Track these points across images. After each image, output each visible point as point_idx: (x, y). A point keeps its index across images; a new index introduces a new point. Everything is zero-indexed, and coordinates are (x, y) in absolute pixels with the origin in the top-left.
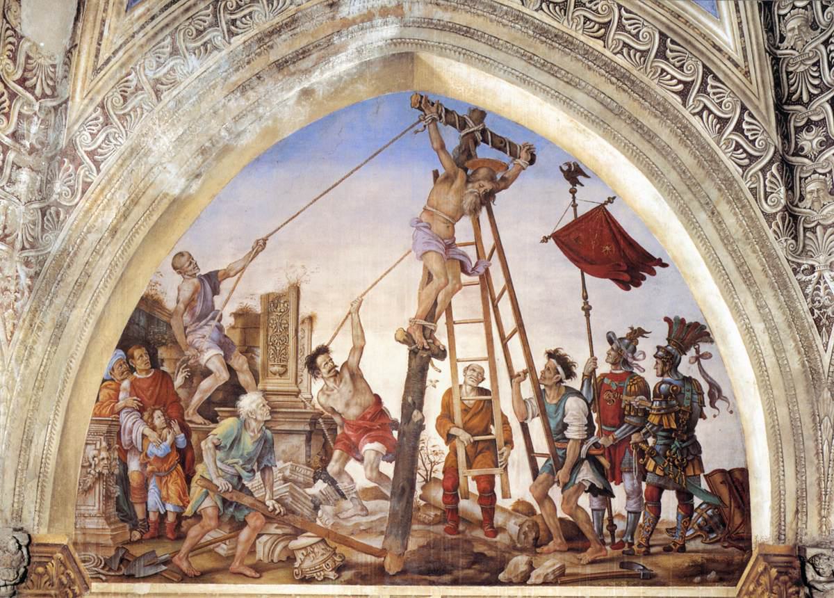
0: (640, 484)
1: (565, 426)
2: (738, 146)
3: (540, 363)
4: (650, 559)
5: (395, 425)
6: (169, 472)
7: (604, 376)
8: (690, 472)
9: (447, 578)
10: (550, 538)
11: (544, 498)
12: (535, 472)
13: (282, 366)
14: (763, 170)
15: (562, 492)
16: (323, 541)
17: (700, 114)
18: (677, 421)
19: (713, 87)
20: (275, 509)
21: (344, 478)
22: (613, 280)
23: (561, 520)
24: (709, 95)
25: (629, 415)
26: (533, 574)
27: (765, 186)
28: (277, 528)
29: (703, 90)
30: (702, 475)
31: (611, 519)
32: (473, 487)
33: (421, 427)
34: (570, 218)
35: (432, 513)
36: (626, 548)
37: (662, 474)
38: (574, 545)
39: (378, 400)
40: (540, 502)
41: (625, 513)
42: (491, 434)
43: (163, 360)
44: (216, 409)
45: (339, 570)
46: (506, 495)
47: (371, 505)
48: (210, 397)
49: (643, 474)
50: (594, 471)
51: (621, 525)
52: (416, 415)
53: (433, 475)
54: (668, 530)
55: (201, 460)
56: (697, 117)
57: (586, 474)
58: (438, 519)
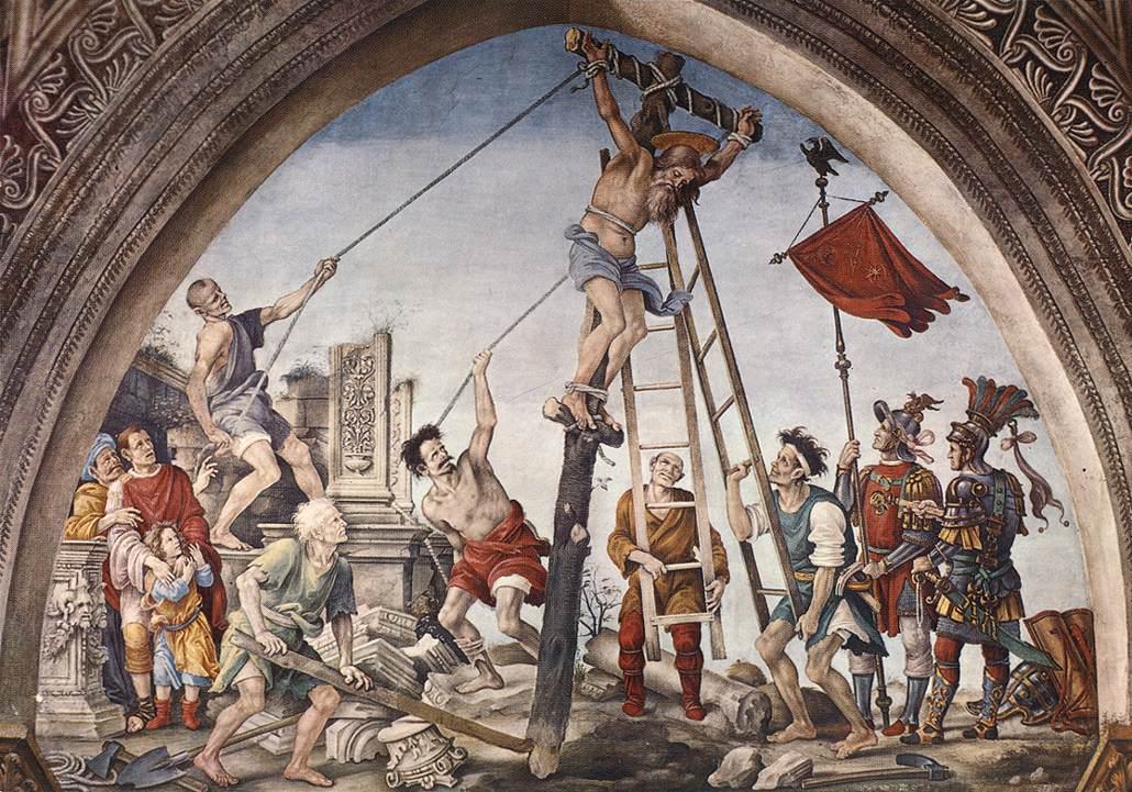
0: (927, 634)
1: (811, 547)
2: (1081, 116)
3: (771, 450)
4: (945, 750)
5: (543, 547)
6: (187, 624)
7: (873, 468)
11: (778, 658)
12: (765, 620)
13: (365, 458)
15: (807, 649)
16: (433, 728)
17: (1021, 66)
18: (982, 538)
19: (1042, 24)
20: (355, 680)
22: (881, 320)
23: (806, 691)
24: (1036, 35)
25: (909, 529)
26: (763, 775)
27: (1122, 178)
28: (358, 709)
29: (1026, 28)
30: (1021, 621)
31: (882, 690)
32: (667, 643)
33: (584, 549)
35: (604, 683)
36: (907, 733)
37: (960, 619)
39: (517, 509)
40: (772, 665)
41: (904, 680)
42: (696, 561)
43: (175, 450)
44: (260, 526)
46: (717, 655)
47: (506, 672)
48: (249, 507)
49: (932, 619)
50: (855, 616)
51: (898, 698)
52: (577, 533)
53: (604, 624)
55: (237, 605)
57: (843, 620)
58: (611, 692)
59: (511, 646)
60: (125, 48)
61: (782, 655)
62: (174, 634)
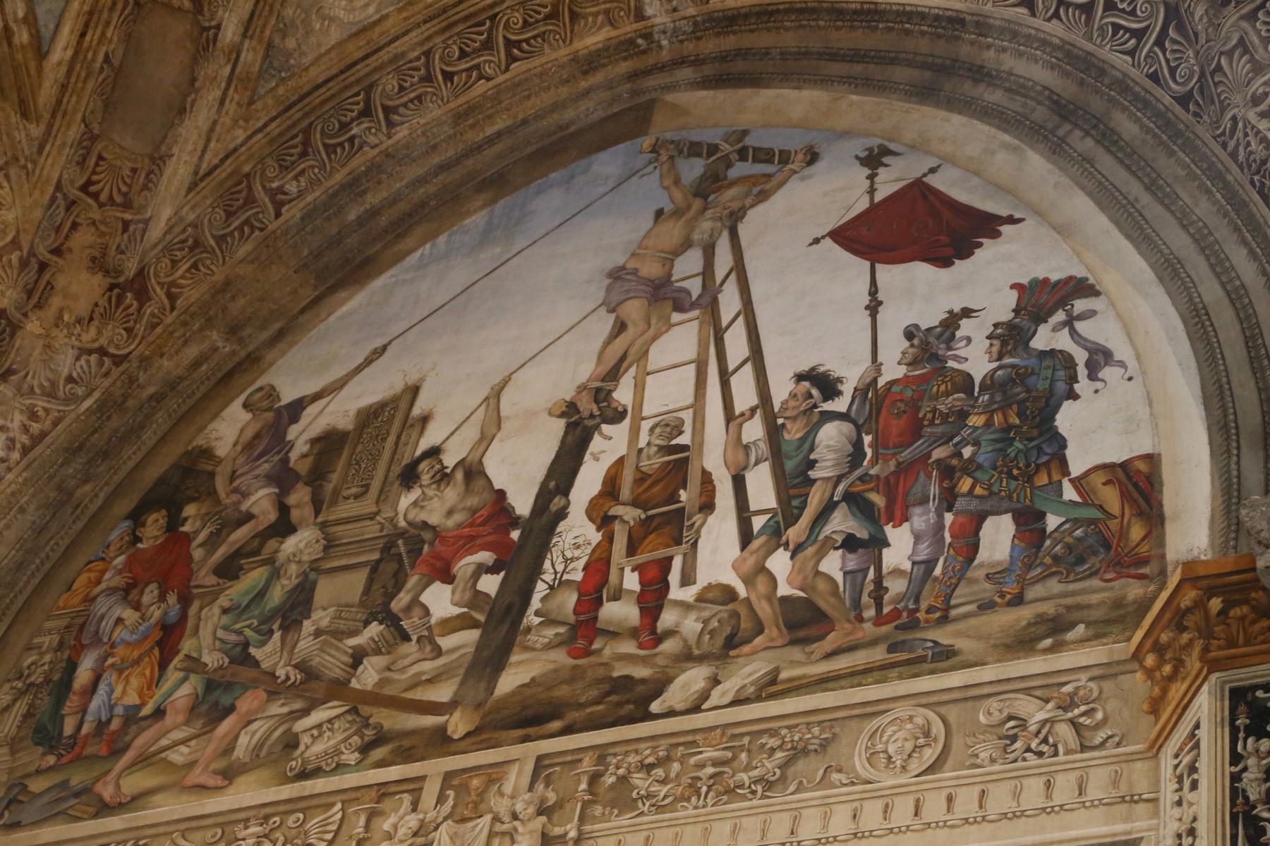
0: (940, 517)
1: (812, 464)
2: (1117, 27)
3: (781, 388)
4: (950, 628)
5: (515, 521)
6: (137, 662)
7: (892, 383)
8: (1042, 479)
9: (556, 725)
10: (759, 629)
12: (746, 537)
13: (363, 486)
14: (1159, 42)
15: (792, 557)
16: (354, 710)
18: (1019, 415)
21: (417, 611)
22: (924, 260)
23: (784, 600)
25: (932, 423)
27: (1167, 61)
28: (283, 705)
31: (878, 581)
32: (632, 581)
33: (562, 514)
34: (863, 204)
35: (550, 632)
37: (985, 493)
38: (801, 634)
39: (501, 494)
40: (748, 581)
41: (907, 566)
42: (680, 502)
43: (186, 519)
44: (242, 562)
45: (365, 749)
46: (687, 580)
48: (240, 548)
49: (949, 500)
50: (854, 515)
51: (896, 587)
52: (558, 502)
53: (565, 577)
54: (988, 577)
56: (1054, 21)
57: (842, 523)
58: (559, 639)
60: (247, 222)
61: (762, 569)
62: (120, 672)
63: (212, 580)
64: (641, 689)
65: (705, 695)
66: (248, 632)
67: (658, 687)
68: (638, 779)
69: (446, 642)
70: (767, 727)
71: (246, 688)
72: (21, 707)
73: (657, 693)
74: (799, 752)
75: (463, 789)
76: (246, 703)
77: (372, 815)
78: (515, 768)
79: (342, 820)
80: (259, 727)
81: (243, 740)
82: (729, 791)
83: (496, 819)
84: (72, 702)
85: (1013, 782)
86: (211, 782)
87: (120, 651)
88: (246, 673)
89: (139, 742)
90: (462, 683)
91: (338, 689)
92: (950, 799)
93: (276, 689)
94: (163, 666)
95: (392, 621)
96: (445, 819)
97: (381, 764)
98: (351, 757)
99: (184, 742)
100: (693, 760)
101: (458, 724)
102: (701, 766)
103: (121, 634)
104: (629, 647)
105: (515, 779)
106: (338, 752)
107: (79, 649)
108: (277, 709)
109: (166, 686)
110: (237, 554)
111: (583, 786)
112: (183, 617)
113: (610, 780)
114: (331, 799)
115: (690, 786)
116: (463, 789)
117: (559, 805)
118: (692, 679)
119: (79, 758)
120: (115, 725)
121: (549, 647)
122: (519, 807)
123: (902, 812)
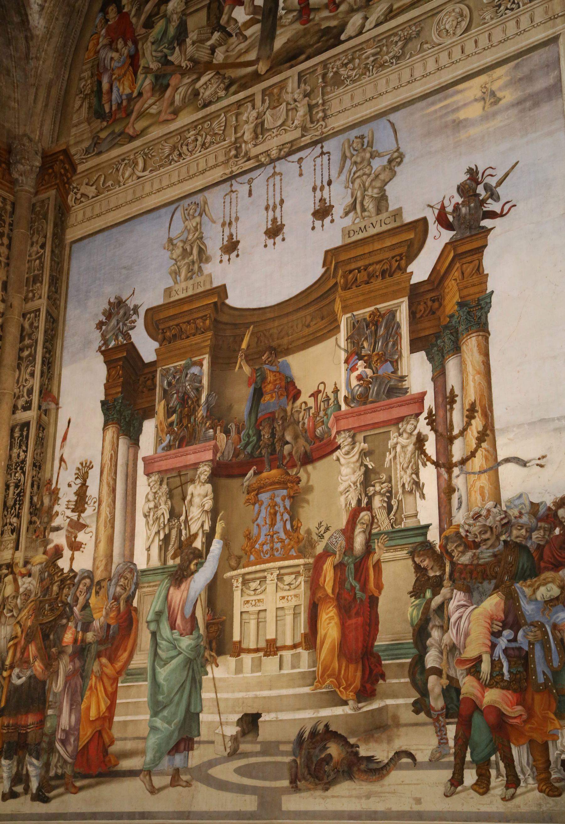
6: (125, 75)
9: (303, 57)
16: (218, 73)
21: (232, 22)
35: (290, 16)
43: (124, 6)
45: (227, 88)
58: (295, 18)
59: (251, 19)
62: (119, 80)
63: (143, 31)
64: (335, 31)
65: (363, 26)
66: (165, 50)
67: (342, 28)
68: (342, 71)
69: (248, 33)
70: (392, 32)
71: (171, 75)
72: (86, 105)
73: (342, 31)
74: (408, 40)
75: (271, 95)
76: (173, 81)
77: (237, 115)
78: (290, 81)
79: (226, 120)
80: (182, 90)
81: (177, 97)
82: (382, 66)
83: (288, 104)
84: (105, 98)
85: (502, 26)
86: (170, 117)
87: (116, 71)
88: (170, 69)
89: (137, 108)
90: (259, 49)
91: (209, 66)
92: (476, 42)
93: (184, 72)
94: (135, 73)
95: (222, 29)
96: (267, 109)
97: (235, 93)
98: (222, 93)
99: (154, 104)
100: (363, 57)
101: (262, 68)
102: (368, 58)
103: (114, 64)
104: (325, 13)
105: (292, 85)
106: (216, 93)
107: (100, 75)
108: (187, 80)
109: (139, 82)
110: (150, 17)
111: (320, 80)
112: (137, 50)
113: (331, 75)
114: (219, 113)
115: (365, 68)
116: (271, 95)
117: (312, 91)
118: (356, 20)
119: (115, 121)
120: (125, 103)
121: (292, 23)
122: (296, 96)
123: (457, 54)
